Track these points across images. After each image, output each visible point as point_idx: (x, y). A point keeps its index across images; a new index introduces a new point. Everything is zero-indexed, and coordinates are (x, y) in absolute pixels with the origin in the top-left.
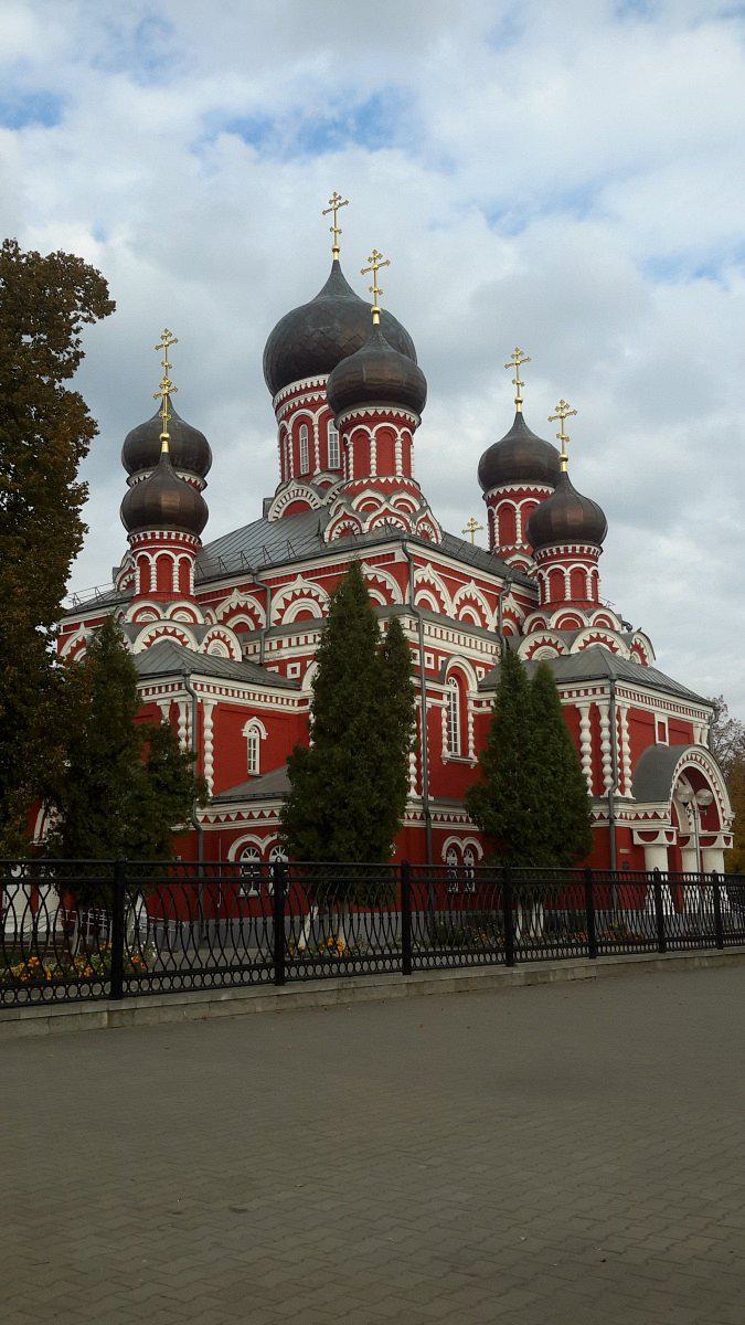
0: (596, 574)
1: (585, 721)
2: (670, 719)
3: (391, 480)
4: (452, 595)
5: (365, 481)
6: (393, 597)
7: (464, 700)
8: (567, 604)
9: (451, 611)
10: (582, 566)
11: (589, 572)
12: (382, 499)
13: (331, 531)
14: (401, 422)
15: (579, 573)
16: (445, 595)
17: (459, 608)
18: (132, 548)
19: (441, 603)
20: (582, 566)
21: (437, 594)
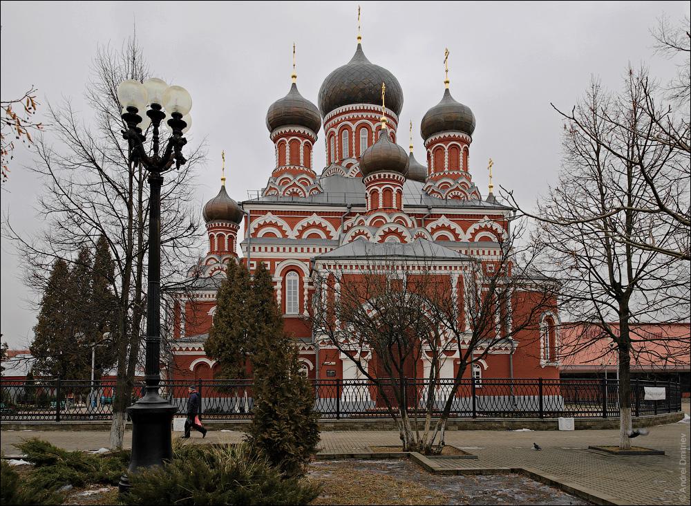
0: (399, 192)
3: (297, 168)
6: (283, 229)
7: (302, 283)
10: (391, 187)
11: (395, 191)
12: (292, 179)
14: (303, 136)
15: (388, 191)
18: (208, 230)
20: (391, 187)
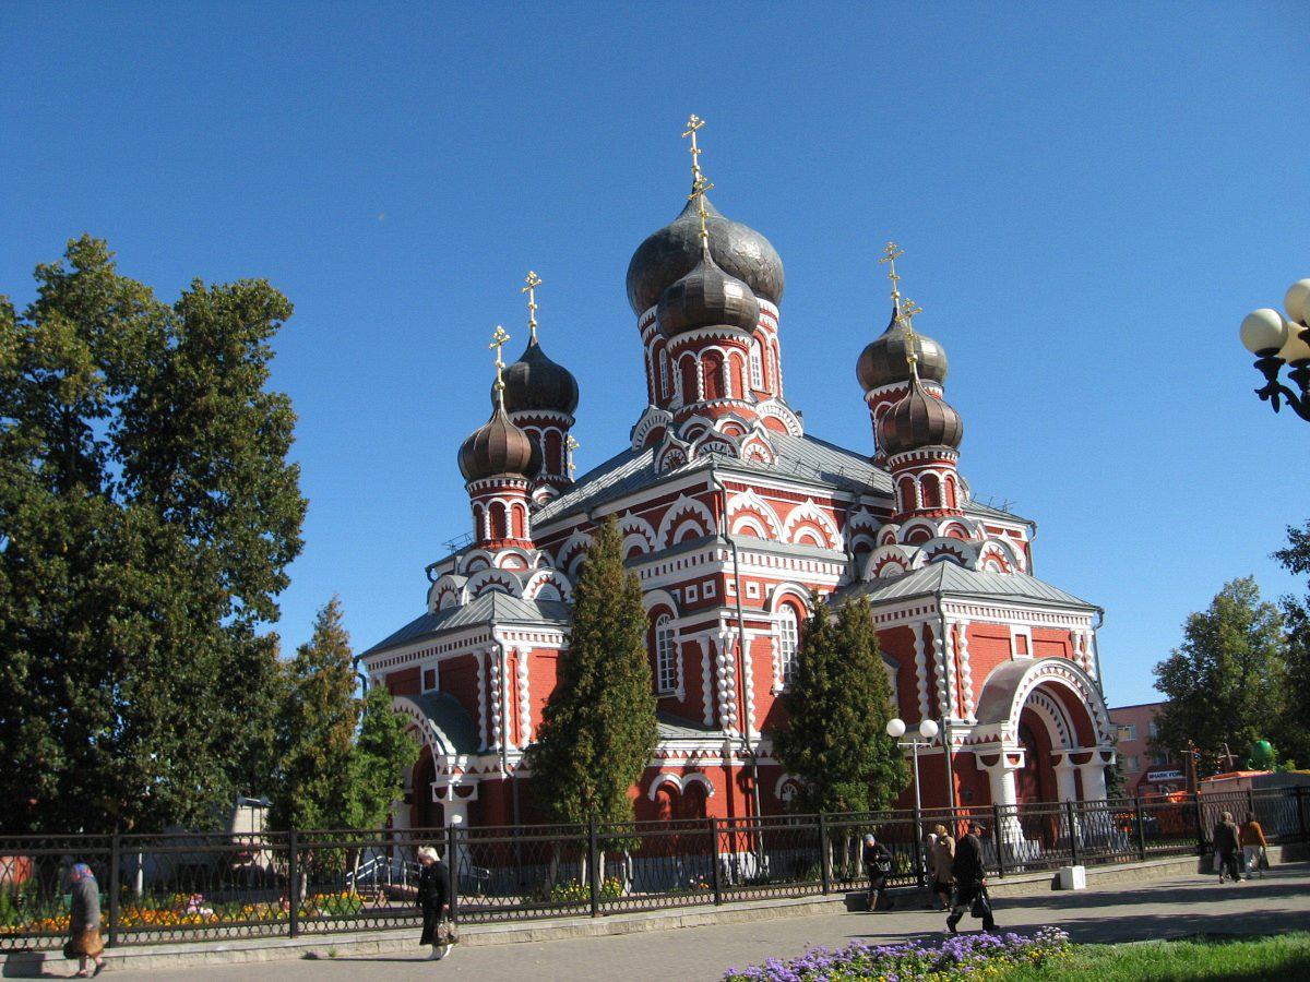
1: (919, 645)
2: (1033, 628)
4: (782, 516)
5: (692, 407)
8: (918, 513)
9: (783, 533)
13: (661, 462)
16: (773, 519)
17: (793, 530)
19: (768, 528)
21: (763, 519)
